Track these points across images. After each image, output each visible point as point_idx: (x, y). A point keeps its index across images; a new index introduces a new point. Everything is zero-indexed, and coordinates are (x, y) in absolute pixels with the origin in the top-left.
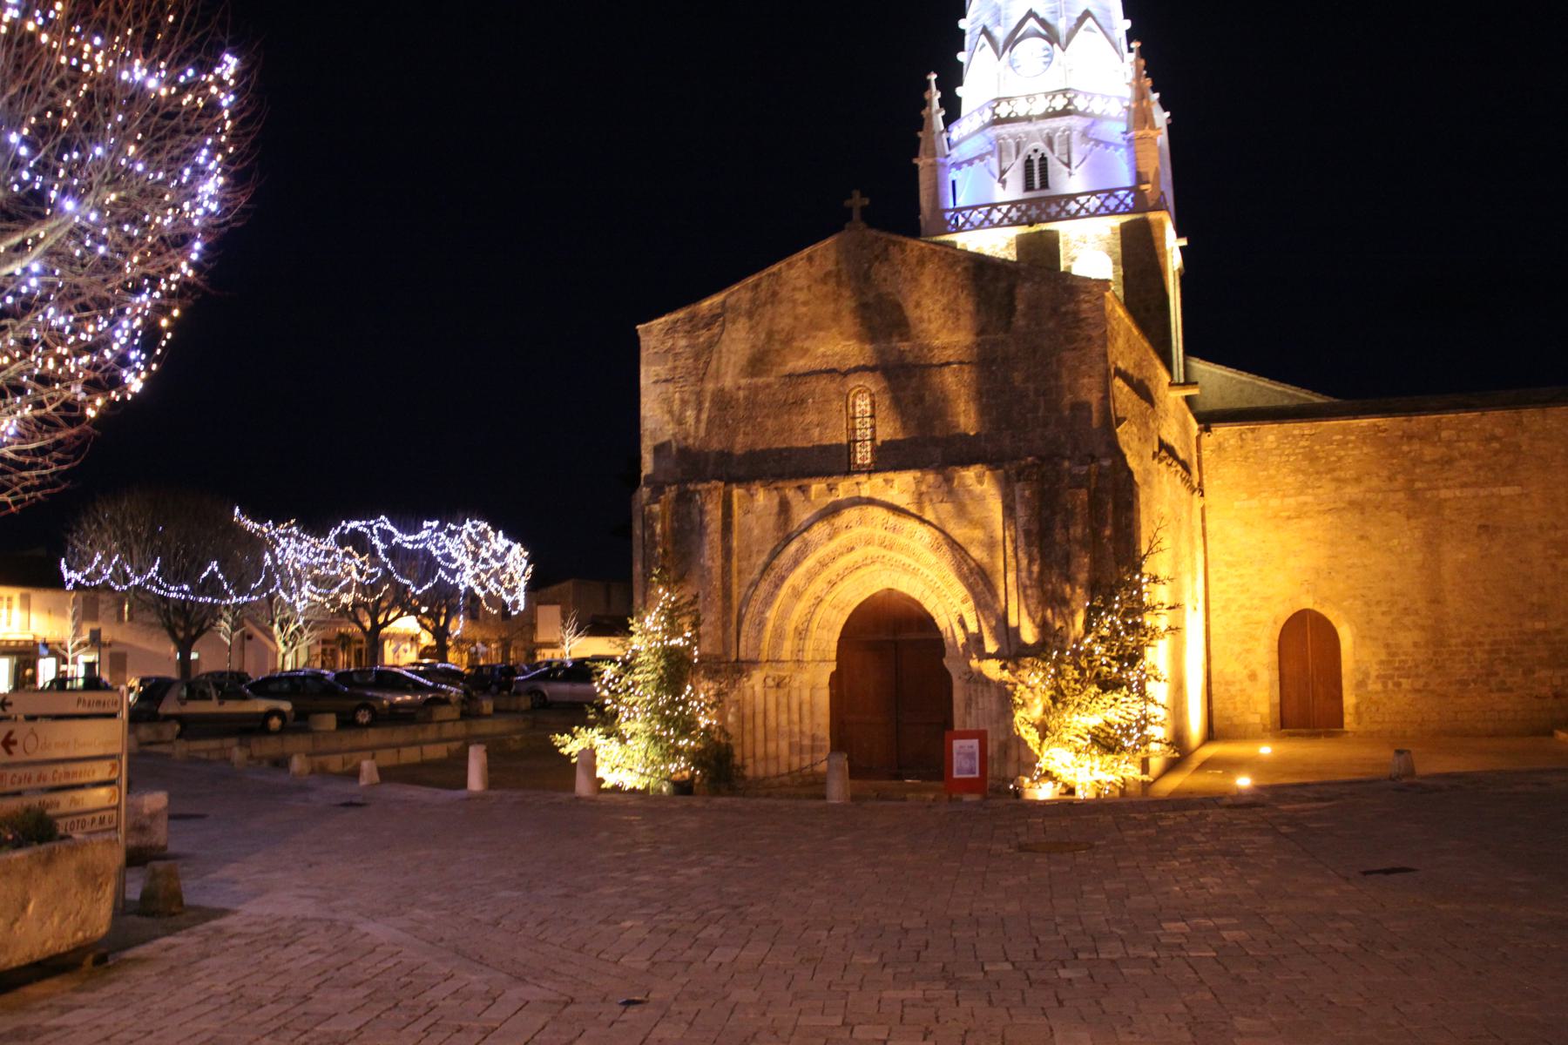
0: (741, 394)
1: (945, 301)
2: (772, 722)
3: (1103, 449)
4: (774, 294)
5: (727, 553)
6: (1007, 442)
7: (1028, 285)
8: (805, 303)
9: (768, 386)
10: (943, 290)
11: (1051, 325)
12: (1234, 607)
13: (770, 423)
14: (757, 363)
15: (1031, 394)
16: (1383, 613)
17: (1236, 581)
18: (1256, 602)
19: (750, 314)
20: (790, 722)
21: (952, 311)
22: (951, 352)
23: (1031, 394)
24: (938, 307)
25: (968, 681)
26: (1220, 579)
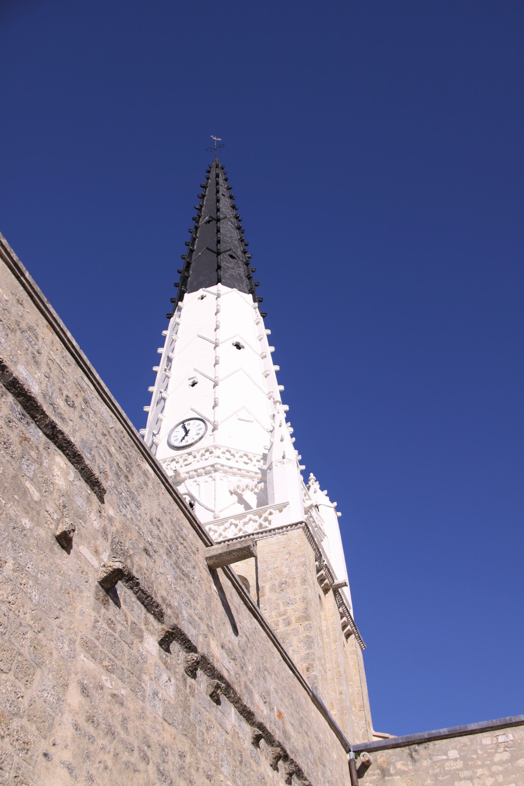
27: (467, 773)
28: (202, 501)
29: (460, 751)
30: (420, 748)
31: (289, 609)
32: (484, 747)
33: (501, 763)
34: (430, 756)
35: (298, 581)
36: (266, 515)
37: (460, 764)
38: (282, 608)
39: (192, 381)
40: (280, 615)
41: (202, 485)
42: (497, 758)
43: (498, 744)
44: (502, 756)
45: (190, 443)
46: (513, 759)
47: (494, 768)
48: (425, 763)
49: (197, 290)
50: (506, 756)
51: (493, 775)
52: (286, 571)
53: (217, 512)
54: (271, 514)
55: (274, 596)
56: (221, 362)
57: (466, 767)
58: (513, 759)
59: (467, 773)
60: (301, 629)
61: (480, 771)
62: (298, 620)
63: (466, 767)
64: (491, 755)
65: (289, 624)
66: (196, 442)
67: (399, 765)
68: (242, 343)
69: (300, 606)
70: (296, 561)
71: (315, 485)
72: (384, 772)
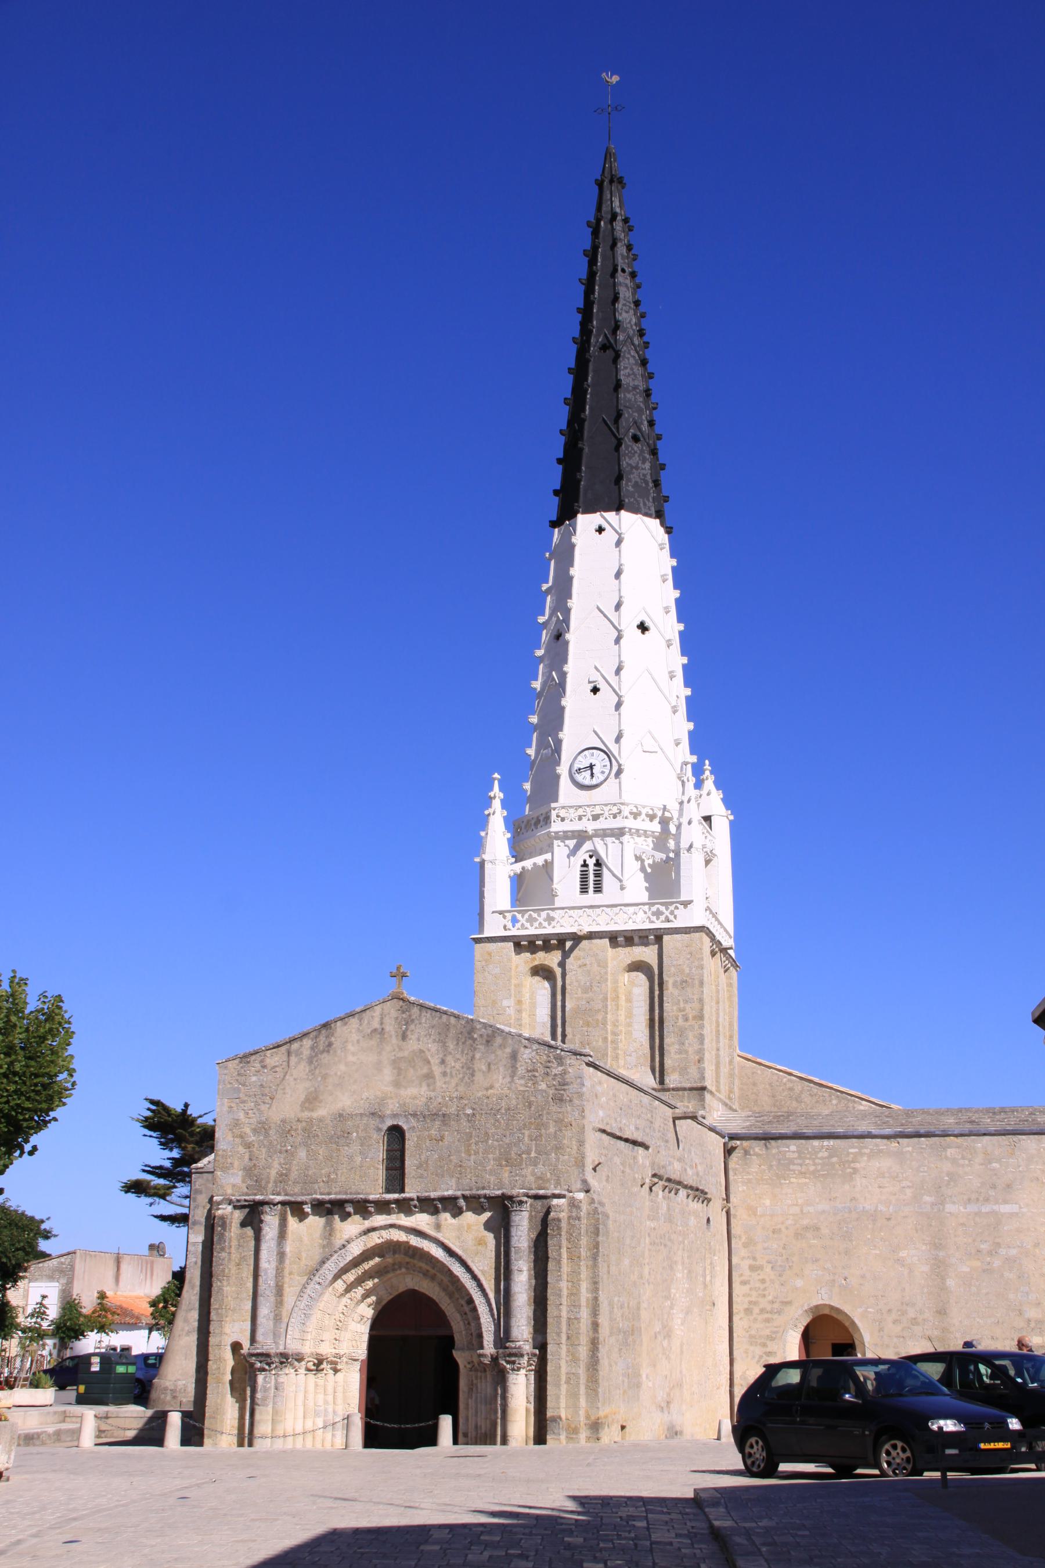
0: (300, 1126)
1: (463, 1060)
2: (311, 1403)
3: (579, 1185)
4: (330, 1045)
5: (281, 1255)
6: (506, 1175)
7: (528, 1051)
8: (353, 1054)
9: (321, 1120)
10: (462, 1052)
11: (543, 1086)
12: (756, 1310)
13: (322, 1151)
14: (311, 1100)
15: (526, 1139)
16: (895, 1322)
17: (758, 1285)
18: (776, 1306)
19: (310, 1061)
20: (326, 1402)
21: (469, 1068)
22: (466, 1102)
23: (526, 1139)
24: (458, 1065)
25: (471, 1370)
26: (744, 1283)
27: (799, 1161)
28: (609, 865)
29: (798, 1147)
30: (773, 1142)
31: (688, 1006)
32: (813, 1147)
33: (822, 1158)
34: (778, 1147)
35: (697, 982)
36: (672, 908)
37: (796, 1155)
38: (682, 1005)
39: (592, 685)
40: (680, 1010)
41: (610, 846)
42: (820, 1155)
43: (823, 1146)
44: (824, 1154)
45: (594, 782)
46: (830, 1156)
47: (817, 1161)
48: (774, 1151)
49: (594, 511)
50: (826, 1154)
51: (815, 1164)
52: (687, 971)
53: (624, 879)
54: (676, 908)
55: (676, 992)
56: (626, 665)
57: (800, 1157)
58: (830, 1156)
59: (799, 1161)
60: (696, 1027)
61: (807, 1161)
62: (694, 1018)
63: (800, 1157)
64: (817, 1153)
65: (687, 1020)
66: (601, 783)
67: (757, 1150)
68: (648, 623)
69: (696, 1005)
70: (696, 963)
71: (709, 784)
72: (746, 1152)
